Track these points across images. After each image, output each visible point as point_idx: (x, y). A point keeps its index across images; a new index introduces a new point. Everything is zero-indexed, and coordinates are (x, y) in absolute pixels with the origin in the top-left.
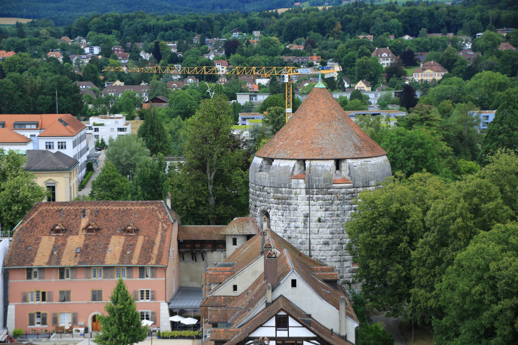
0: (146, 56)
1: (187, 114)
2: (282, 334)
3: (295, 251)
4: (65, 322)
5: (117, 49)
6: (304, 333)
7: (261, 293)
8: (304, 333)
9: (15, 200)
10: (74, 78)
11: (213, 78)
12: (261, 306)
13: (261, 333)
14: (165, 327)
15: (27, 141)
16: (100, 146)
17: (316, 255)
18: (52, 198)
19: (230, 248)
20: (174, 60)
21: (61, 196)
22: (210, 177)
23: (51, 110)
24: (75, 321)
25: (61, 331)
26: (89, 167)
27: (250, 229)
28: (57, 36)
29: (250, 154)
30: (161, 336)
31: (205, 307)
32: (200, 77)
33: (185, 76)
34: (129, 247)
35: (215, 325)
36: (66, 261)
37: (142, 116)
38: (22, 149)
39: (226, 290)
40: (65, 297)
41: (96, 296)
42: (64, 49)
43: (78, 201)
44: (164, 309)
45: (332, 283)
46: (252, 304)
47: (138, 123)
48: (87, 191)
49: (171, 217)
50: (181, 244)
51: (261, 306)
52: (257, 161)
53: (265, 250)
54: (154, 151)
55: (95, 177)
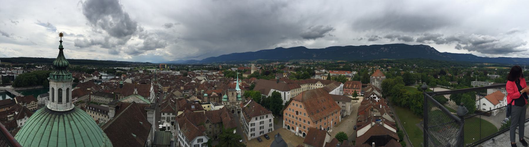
0: (358, 65)
1: (363, 71)
2: (374, 96)
3: (375, 87)
4: (349, 94)
5: (356, 64)
6: (376, 96)
7: (371, 92)
8: (376, 96)
9: (345, 80)
10: (351, 67)
11: (366, 67)
12: (371, 93)
13: (371, 96)
14: (360, 95)
15: (346, 74)
16: (353, 75)
17: (377, 87)
18: (348, 80)
19: (368, 87)
20: (362, 65)
21: (349, 80)
22: (366, 78)
23: (348, 71)
24: (350, 94)
25: (349, 95)
26: (352, 77)
27: (370, 84)
28: (349, 63)
29: (370, 76)
30: (360, 96)
31: (364, 93)
32: (365, 67)
33: (363, 67)
34: (356, 86)
35: (366, 95)
36: (349, 87)
37: (358, 71)
38: (345, 75)
39: (367, 91)
40: (349, 91)
41: (353, 91)
42: (350, 64)
43: (351, 81)
44: (360, 93)
45: (379, 91)
46: (370, 93)
47: (358, 72)
48: (352, 80)
49: (361, 83)
50: (362, 86)
51: (371, 93)
52: (371, 77)
53: (372, 87)
54: (359, 75)
55: (353, 78)
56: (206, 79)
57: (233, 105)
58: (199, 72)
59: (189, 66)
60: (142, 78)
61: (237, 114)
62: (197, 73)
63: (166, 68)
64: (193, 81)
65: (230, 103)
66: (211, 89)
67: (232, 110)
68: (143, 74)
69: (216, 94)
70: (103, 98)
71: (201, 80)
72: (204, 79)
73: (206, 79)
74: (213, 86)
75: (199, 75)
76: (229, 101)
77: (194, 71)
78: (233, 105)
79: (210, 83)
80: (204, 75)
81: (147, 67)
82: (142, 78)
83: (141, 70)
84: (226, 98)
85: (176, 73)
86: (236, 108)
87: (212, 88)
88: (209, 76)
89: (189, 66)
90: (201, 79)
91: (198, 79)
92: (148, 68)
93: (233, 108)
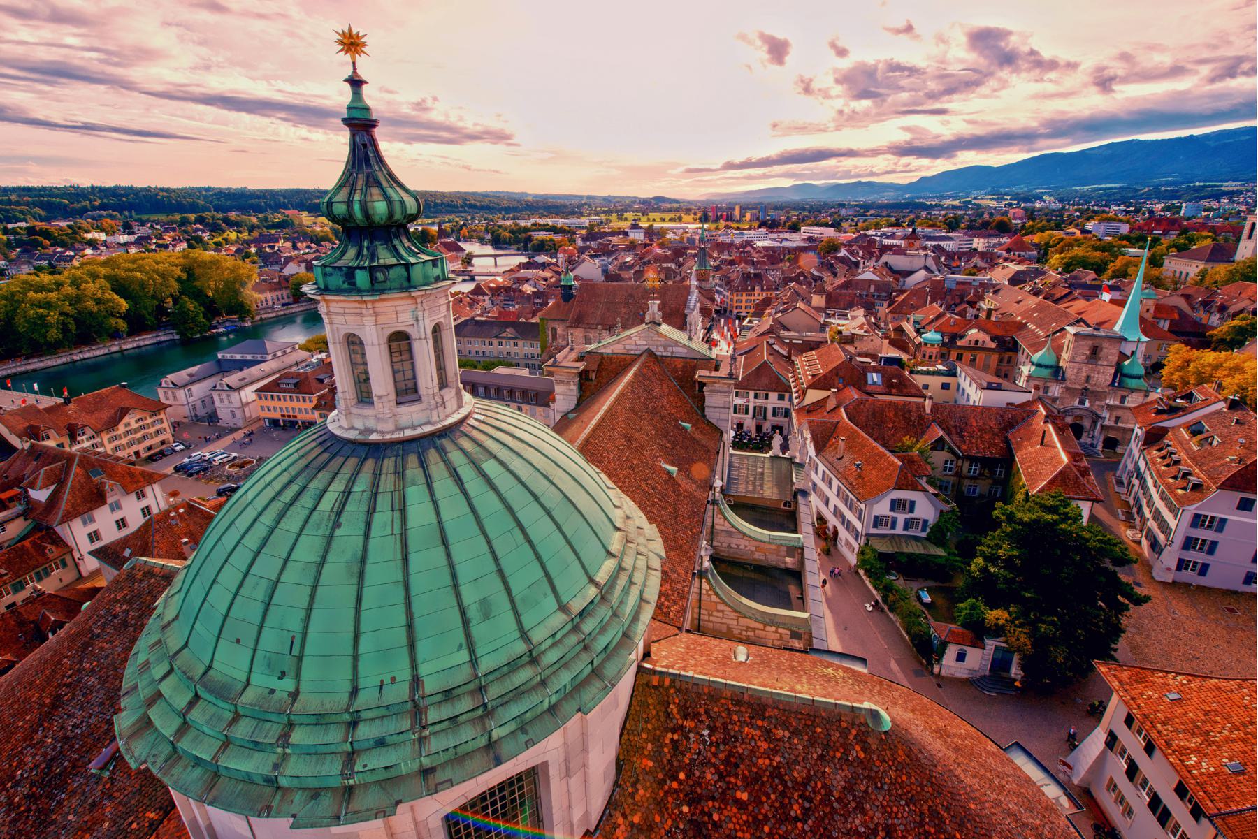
56: (934, 268)
57: (1082, 402)
58: (892, 236)
59: (843, 212)
60: (640, 259)
61: (1100, 447)
62: (886, 241)
63: (738, 218)
64: (868, 275)
65: (1067, 389)
66: (962, 314)
67: (1069, 420)
68: (646, 245)
69: (987, 338)
70: (495, 342)
71: (910, 273)
72: (926, 268)
73: (934, 268)
74: (972, 304)
75: (898, 250)
76: (1064, 379)
77: (870, 232)
78: (1082, 402)
79: (954, 287)
80: (925, 248)
81: (658, 219)
82: (646, 260)
83: (635, 227)
84: (1046, 367)
85: (786, 239)
86: (1096, 418)
87: (965, 310)
88: (951, 256)
89: (843, 212)
90: (909, 269)
91: (890, 268)
92: (663, 220)
93: (1078, 417)
